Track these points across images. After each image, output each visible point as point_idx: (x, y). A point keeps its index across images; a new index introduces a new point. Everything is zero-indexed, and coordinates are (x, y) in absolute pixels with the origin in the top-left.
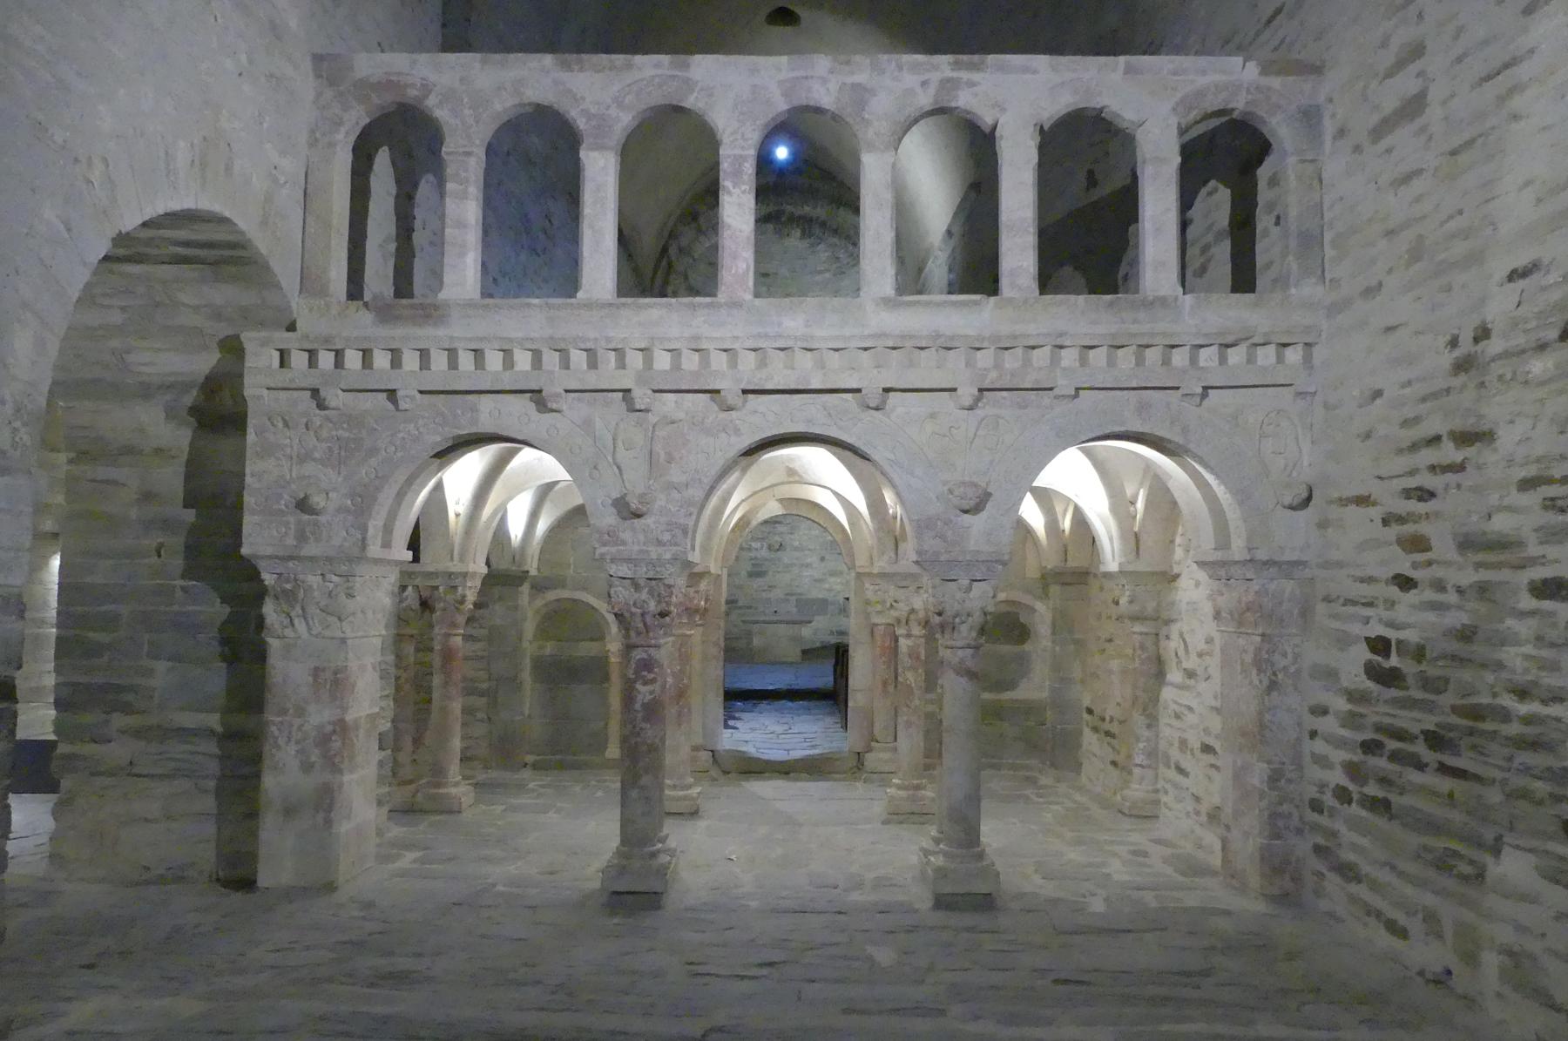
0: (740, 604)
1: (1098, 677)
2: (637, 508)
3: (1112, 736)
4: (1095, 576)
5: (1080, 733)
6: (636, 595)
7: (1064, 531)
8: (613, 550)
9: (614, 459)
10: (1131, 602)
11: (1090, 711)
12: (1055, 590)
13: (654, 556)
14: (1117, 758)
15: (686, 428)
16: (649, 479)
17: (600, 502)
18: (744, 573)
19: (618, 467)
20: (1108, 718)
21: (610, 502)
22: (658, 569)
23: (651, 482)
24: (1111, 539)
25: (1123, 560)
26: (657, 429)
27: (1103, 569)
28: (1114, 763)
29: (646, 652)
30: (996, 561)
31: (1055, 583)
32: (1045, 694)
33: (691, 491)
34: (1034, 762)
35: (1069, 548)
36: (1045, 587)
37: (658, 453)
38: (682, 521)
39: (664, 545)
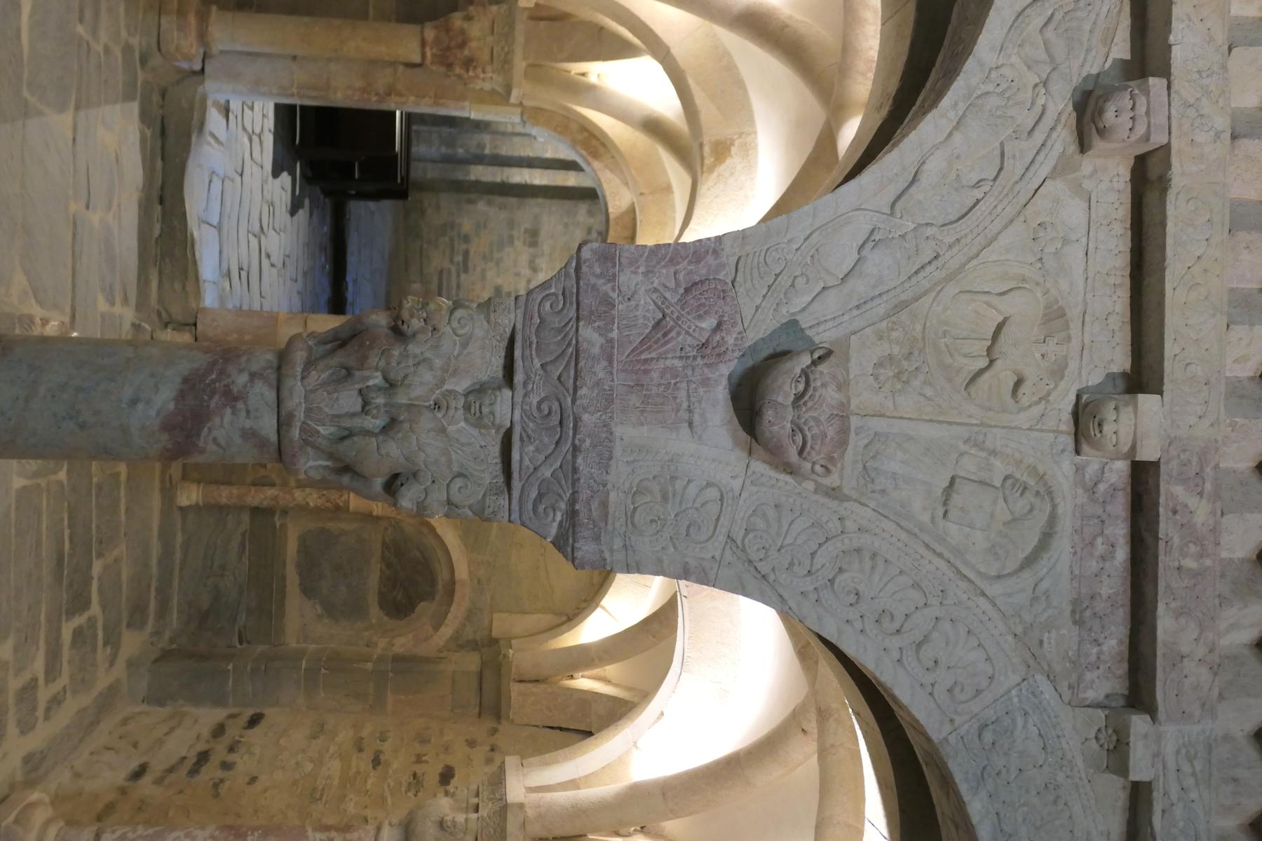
0: (463, 276)
1: (314, 737)
3: (194, 771)
4: (494, 731)
5: (219, 701)
7: (572, 677)
10: (441, 824)
11: (254, 721)
12: (471, 662)
14: (147, 779)
18: (499, 281)
20: (231, 758)
24: (573, 784)
25: (530, 813)
27: (511, 761)
28: (138, 774)
30: (572, 514)
31: (483, 663)
32: (292, 641)
34: (174, 619)
35: (543, 686)
36: (474, 645)
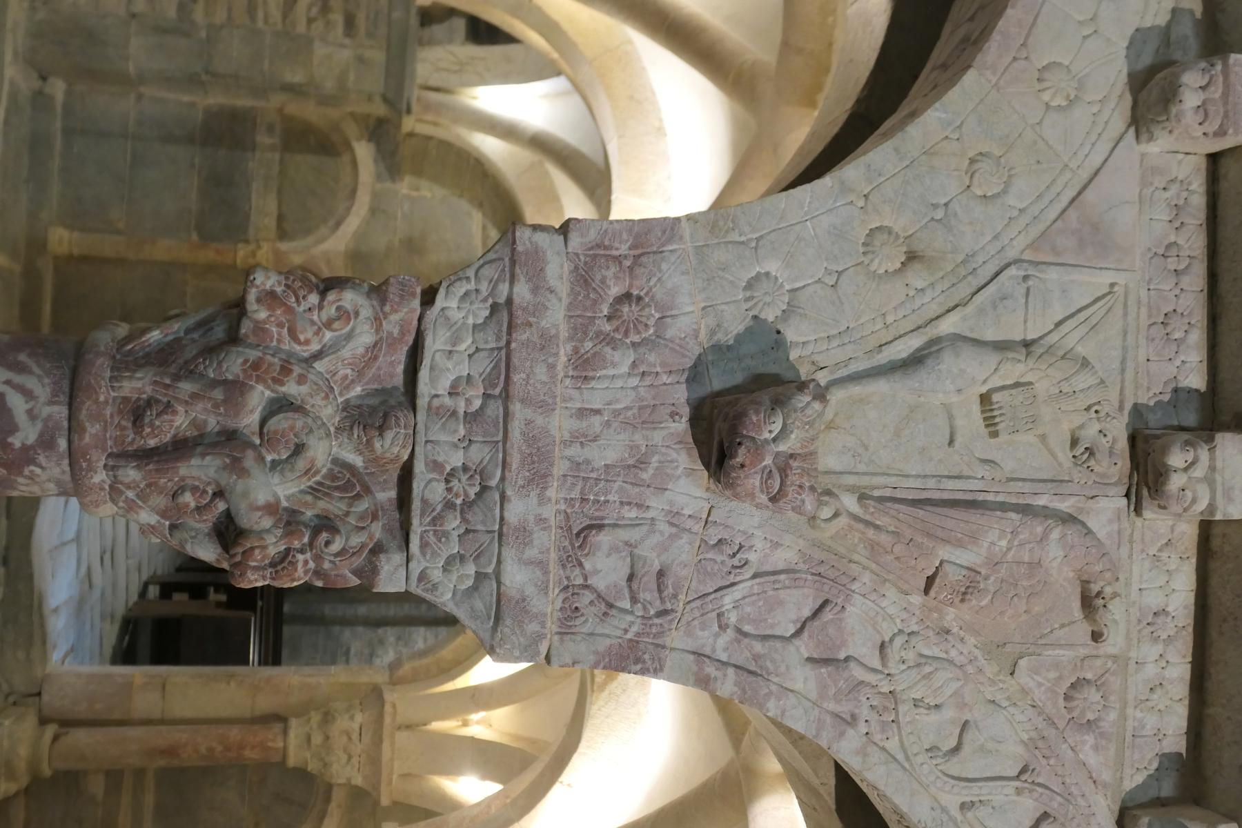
2: (758, 449)
6: (328, 412)
8: (556, 317)
9: (958, 339)
13: (518, 509)
15: (1066, 654)
16: (862, 498)
17: (772, 266)
19: (915, 361)
21: (770, 315)
22: (453, 523)
23: (850, 502)
26: (1072, 533)
29: (46, 442)
33: (803, 679)
37: (974, 538)
38: (676, 639)
39: (571, 560)
